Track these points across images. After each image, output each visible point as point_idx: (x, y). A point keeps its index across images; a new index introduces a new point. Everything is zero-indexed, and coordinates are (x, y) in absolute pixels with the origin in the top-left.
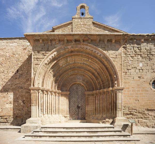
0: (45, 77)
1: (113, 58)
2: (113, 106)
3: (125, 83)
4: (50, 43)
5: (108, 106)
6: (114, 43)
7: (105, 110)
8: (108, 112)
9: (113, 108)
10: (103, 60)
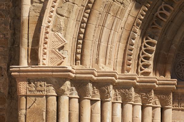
0: (96, 12)
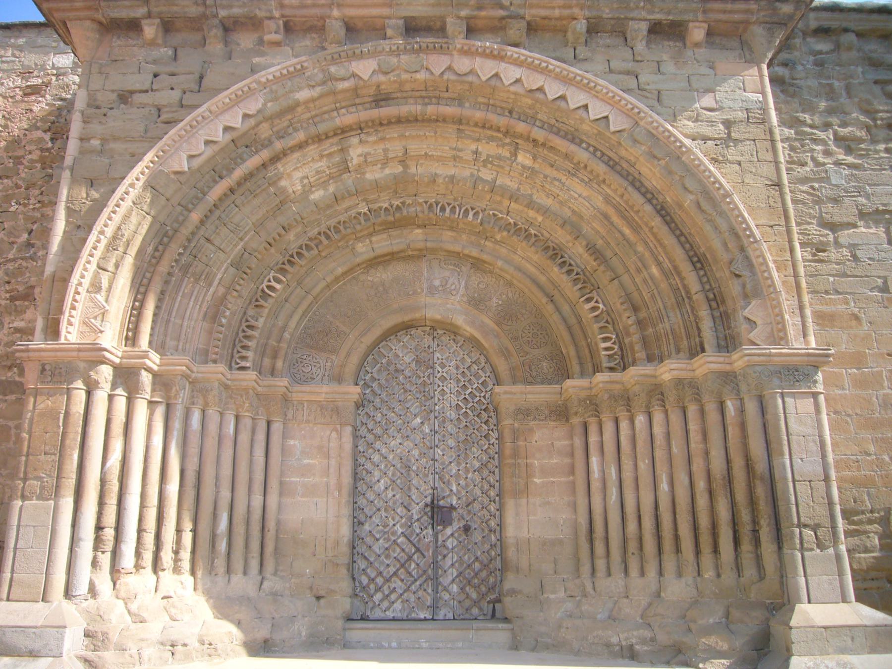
1: (705, 139)
2: (752, 502)
3: (824, 319)
4: (216, 47)
5: (702, 502)
6: (697, 45)
7: (677, 538)
8: (707, 558)
9: (755, 522)
10: (634, 153)
